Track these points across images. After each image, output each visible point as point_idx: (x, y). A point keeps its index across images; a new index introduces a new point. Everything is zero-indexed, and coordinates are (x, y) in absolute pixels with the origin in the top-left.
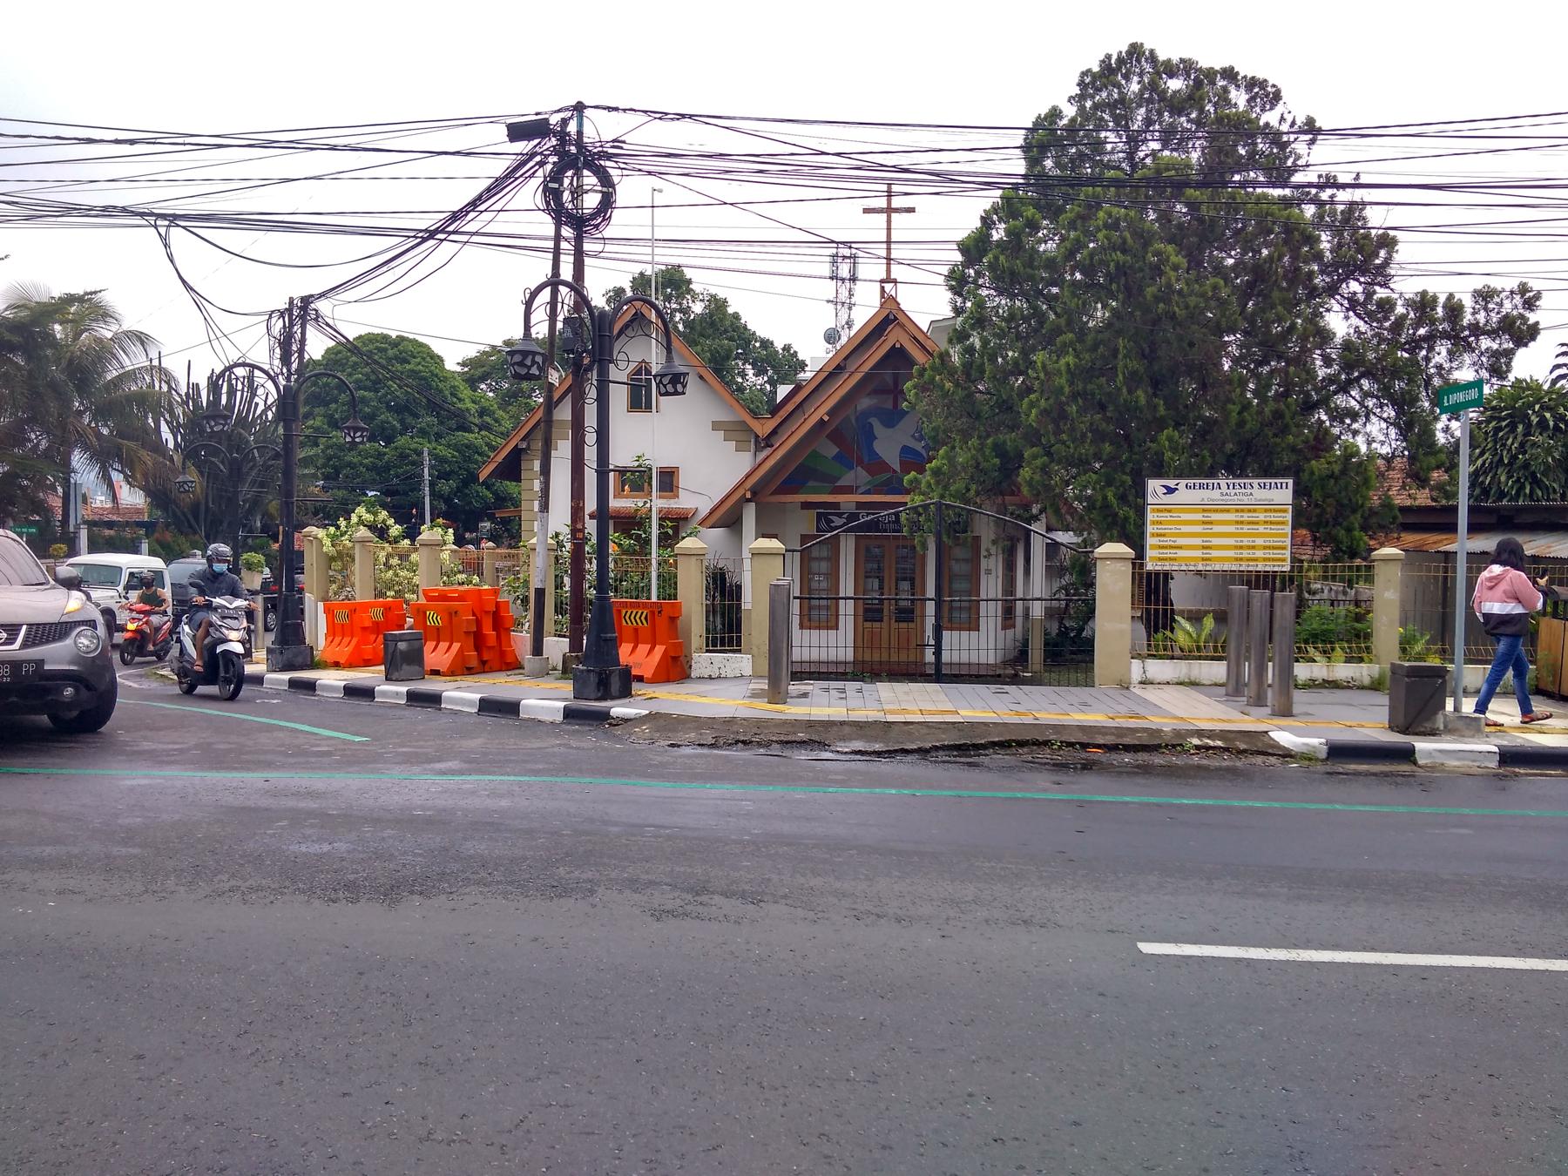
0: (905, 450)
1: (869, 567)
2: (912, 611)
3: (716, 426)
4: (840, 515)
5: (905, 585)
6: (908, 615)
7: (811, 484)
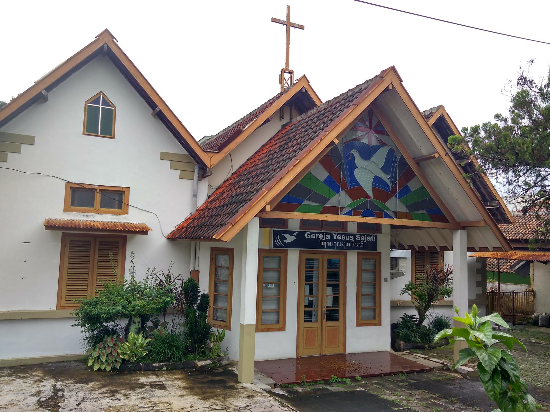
0: (377, 180)
1: (308, 278)
2: (337, 312)
3: (164, 156)
4: (291, 233)
5: (329, 291)
6: (334, 314)
7: (306, 202)
